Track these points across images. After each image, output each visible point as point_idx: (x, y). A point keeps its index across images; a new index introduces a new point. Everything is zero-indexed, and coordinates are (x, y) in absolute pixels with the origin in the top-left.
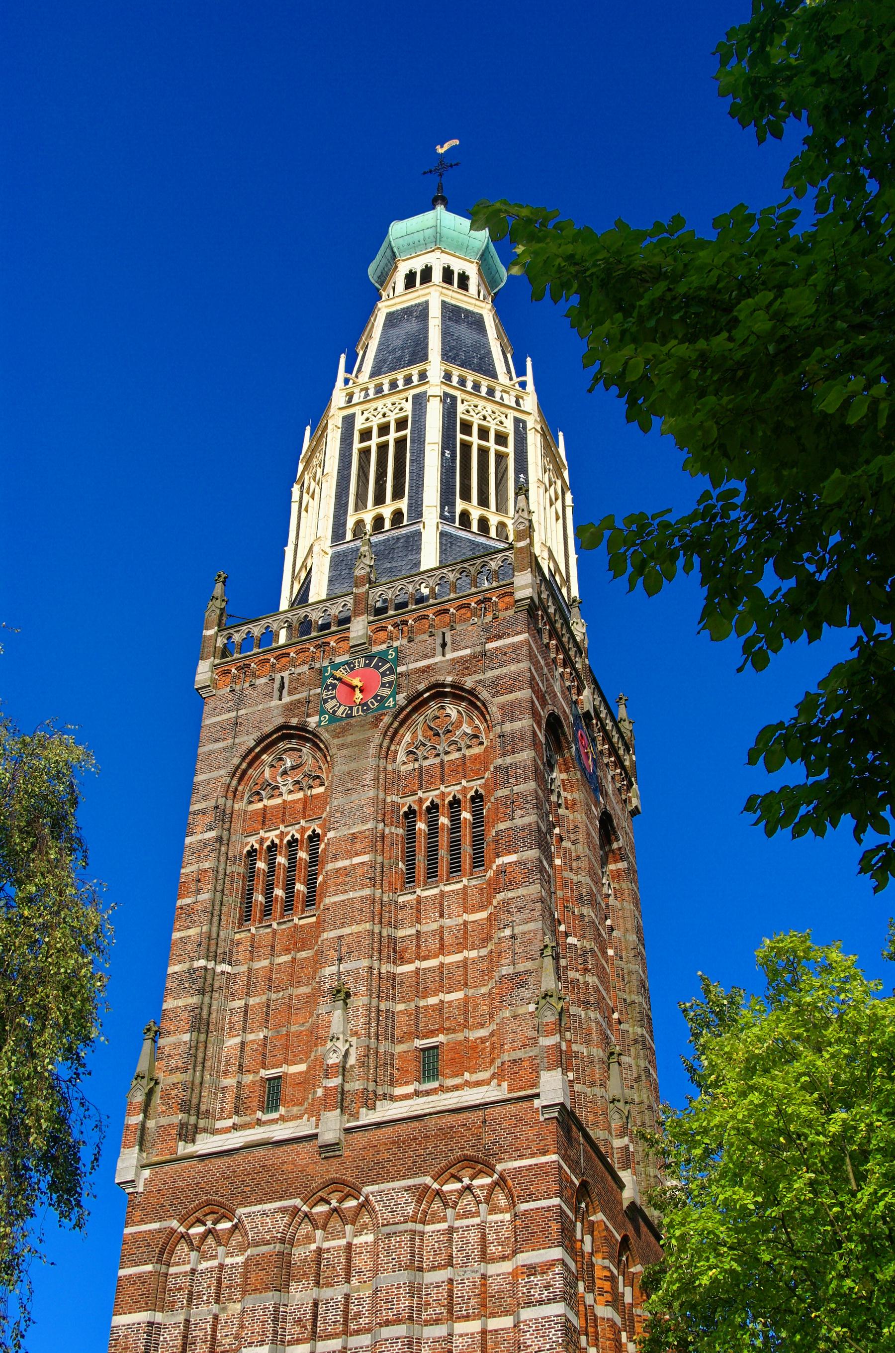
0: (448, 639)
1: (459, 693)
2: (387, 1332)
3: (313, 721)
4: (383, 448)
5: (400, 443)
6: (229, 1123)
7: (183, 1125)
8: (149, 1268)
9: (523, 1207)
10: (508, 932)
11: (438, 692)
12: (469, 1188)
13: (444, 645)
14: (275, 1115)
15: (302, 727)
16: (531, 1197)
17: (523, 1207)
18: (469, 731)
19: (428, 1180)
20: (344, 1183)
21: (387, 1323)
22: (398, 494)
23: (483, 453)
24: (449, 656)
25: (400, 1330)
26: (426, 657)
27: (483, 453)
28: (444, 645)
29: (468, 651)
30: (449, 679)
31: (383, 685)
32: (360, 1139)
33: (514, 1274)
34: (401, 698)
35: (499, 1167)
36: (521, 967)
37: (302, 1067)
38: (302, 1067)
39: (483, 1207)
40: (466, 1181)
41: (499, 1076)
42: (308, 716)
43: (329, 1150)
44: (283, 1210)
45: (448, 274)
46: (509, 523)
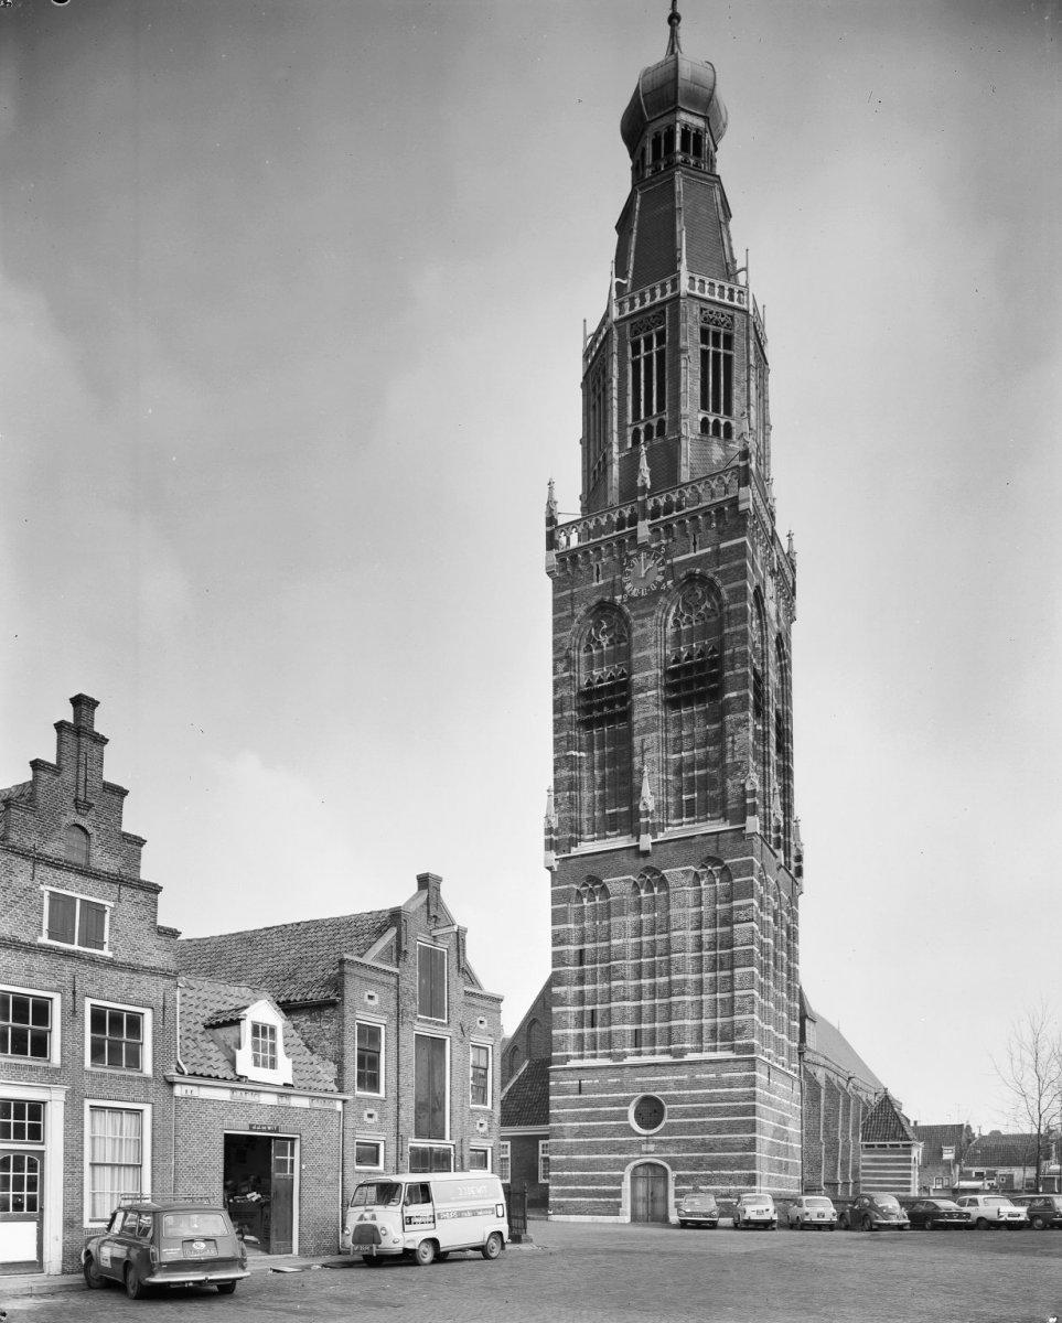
0: (697, 540)
1: (702, 579)
2: (675, 934)
3: (618, 598)
4: (648, 360)
5: (661, 355)
6: (591, 836)
7: (571, 839)
8: (565, 905)
9: (736, 880)
10: (730, 739)
11: (691, 578)
12: (710, 871)
13: (695, 544)
14: (614, 833)
15: (612, 603)
16: (740, 876)
17: (736, 880)
18: (709, 606)
19: (693, 868)
20: (655, 869)
21: (675, 930)
22: (661, 407)
23: (716, 355)
24: (698, 553)
25: (680, 933)
26: (684, 553)
27: (716, 355)
28: (695, 544)
29: (709, 550)
30: (698, 570)
31: (659, 574)
32: (660, 847)
33: (732, 909)
34: (669, 583)
35: (726, 862)
36: (736, 759)
37: (626, 809)
38: (626, 809)
39: (718, 880)
40: (709, 868)
41: (725, 816)
42: (614, 594)
43: (646, 854)
44: (624, 881)
45: (685, 133)
46: (733, 424)
